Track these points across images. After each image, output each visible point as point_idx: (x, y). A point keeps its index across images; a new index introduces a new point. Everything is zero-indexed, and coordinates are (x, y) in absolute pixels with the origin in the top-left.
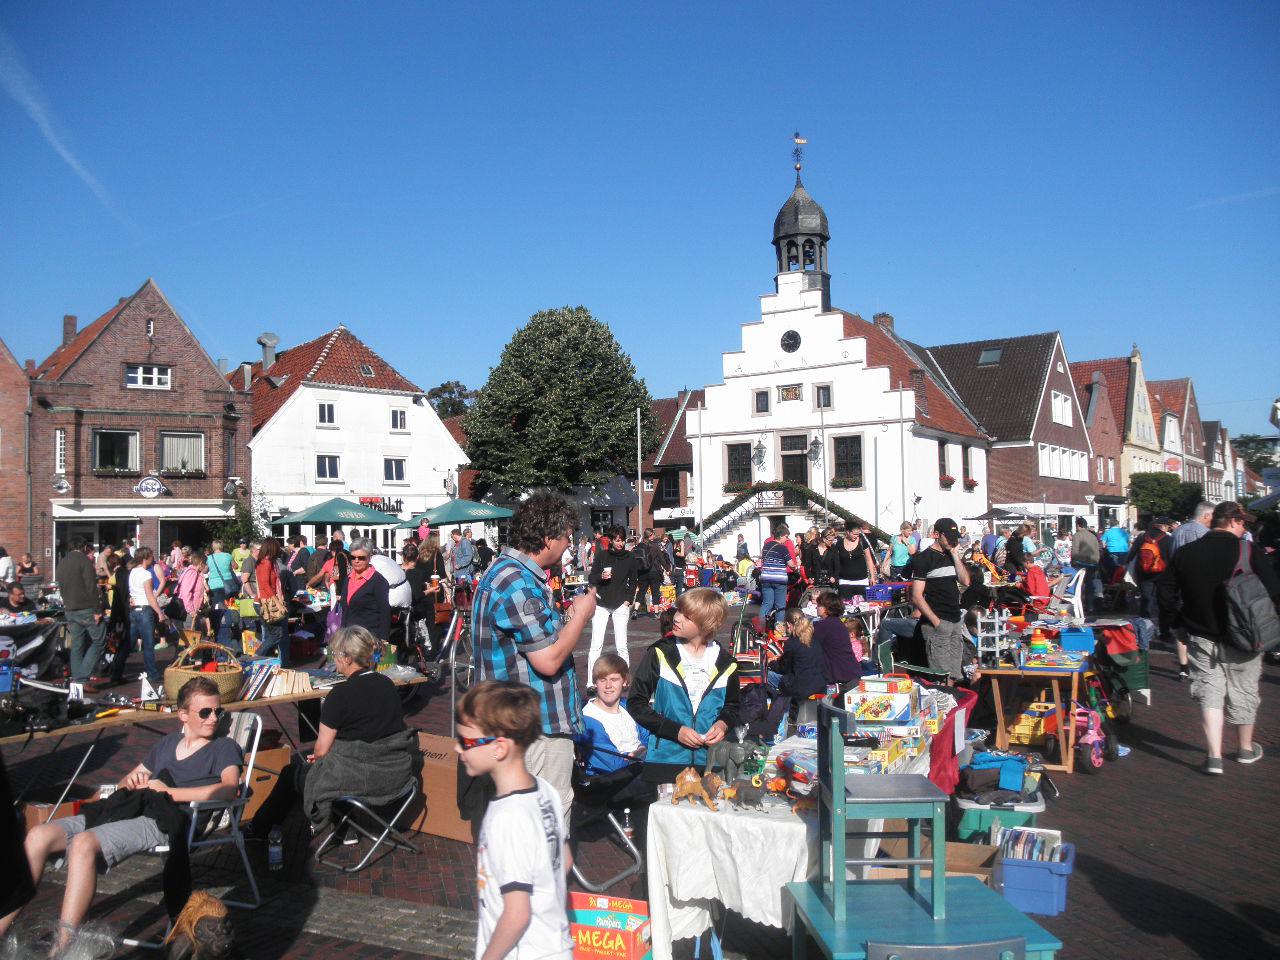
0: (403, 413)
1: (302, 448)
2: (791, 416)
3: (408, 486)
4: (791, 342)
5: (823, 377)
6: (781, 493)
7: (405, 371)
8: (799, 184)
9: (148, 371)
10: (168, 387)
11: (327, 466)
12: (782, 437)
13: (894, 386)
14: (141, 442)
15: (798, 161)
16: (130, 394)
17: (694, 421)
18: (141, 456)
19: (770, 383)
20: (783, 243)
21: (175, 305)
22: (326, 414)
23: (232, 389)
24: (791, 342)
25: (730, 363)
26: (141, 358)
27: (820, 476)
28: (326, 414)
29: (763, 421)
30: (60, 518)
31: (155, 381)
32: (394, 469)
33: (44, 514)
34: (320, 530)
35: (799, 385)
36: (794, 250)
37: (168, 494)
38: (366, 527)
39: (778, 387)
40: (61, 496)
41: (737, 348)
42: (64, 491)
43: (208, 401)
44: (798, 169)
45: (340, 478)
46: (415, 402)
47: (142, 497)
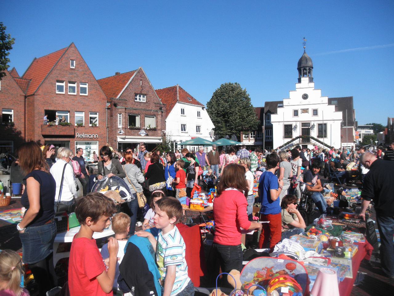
0: (200, 112)
1: (178, 122)
3: (202, 134)
4: (305, 97)
5: (315, 107)
6: (301, 139)
7: (198, 100)
9: (140, 96)
10: (145, 101)
11: (183, 128)
12: (302, 123)
14: (140, 119)
16: (136, 103)
17: (273, 117)
18: (140, 123)
19: (299, 108)
21: (148, 76)
22: (183, 111)
23: (161, 103)
24: (305, 97)
26: (139, 93)
27: (314, 133)
28: (183, 111)
29: (296, 118)
30: (120, 142)
31: (138, 99)
32: (198, 129)
33: (115, 141)
34: (182, 145)
35: (308, 109)
37: (147, 135)
38: (194, 146)
39: (301, 109)
40: (121, 135)
41: (288, 98)
42: (122, 133)
43: (156, 106)
44: (305, 48)
45: (201, 132)
46: (202, 109)
47: (141, 136)
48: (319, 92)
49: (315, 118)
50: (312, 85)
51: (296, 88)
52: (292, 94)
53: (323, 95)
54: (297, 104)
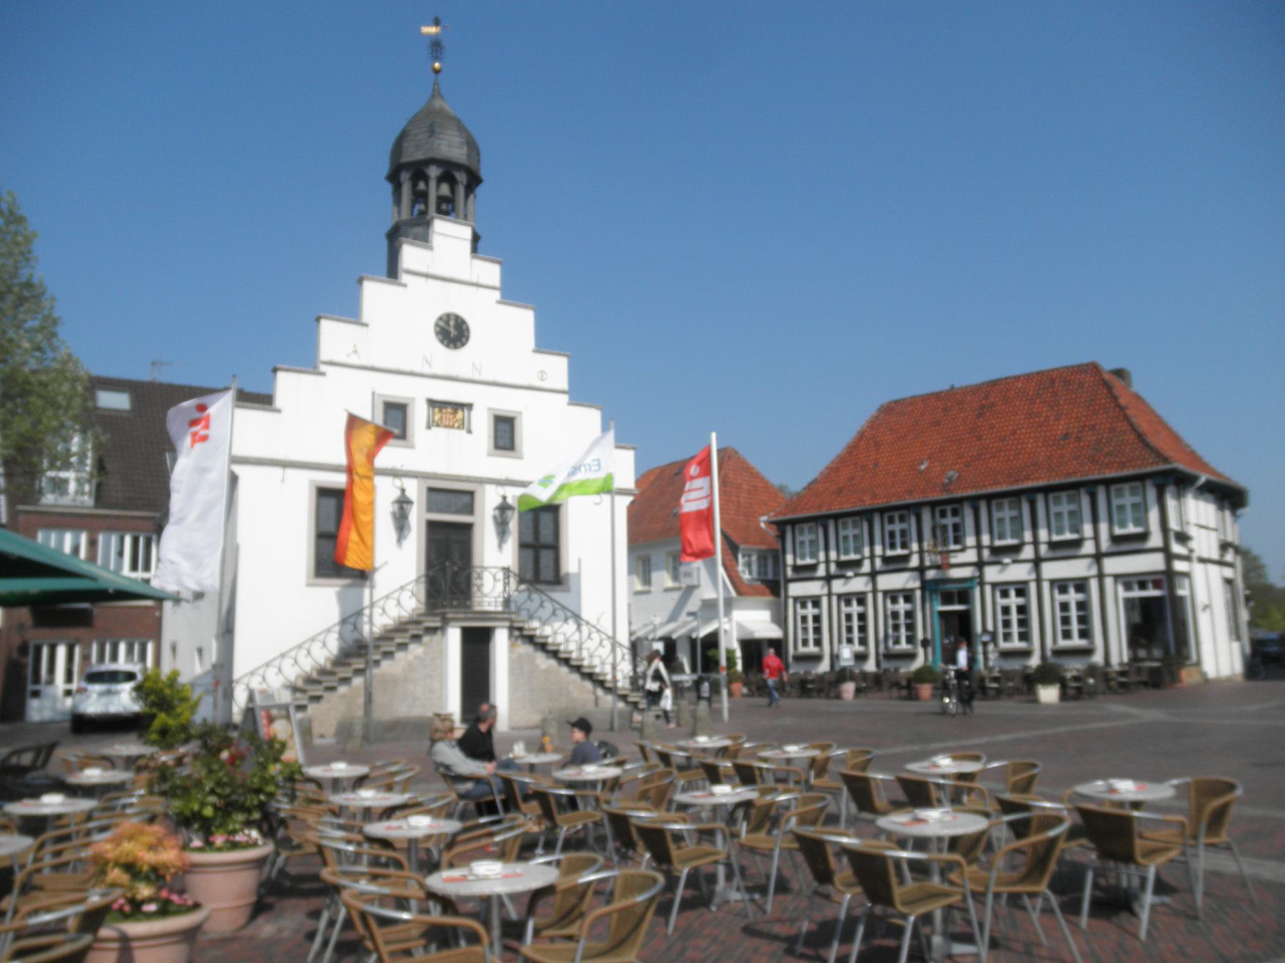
2: (435, 452)
4: (453, 332)
5: (507, 402)
8: (436, 93)
12: (431, 490)
15: (436, 59)
19: (416, 394)
20: (405, 177)
25: (334, 337)
27: (495, 556)
36: (422, 186)
41: (351, 312)
44: (437, 72)
49: (503, 466)
50: (491, 272)
52: (375, 293)
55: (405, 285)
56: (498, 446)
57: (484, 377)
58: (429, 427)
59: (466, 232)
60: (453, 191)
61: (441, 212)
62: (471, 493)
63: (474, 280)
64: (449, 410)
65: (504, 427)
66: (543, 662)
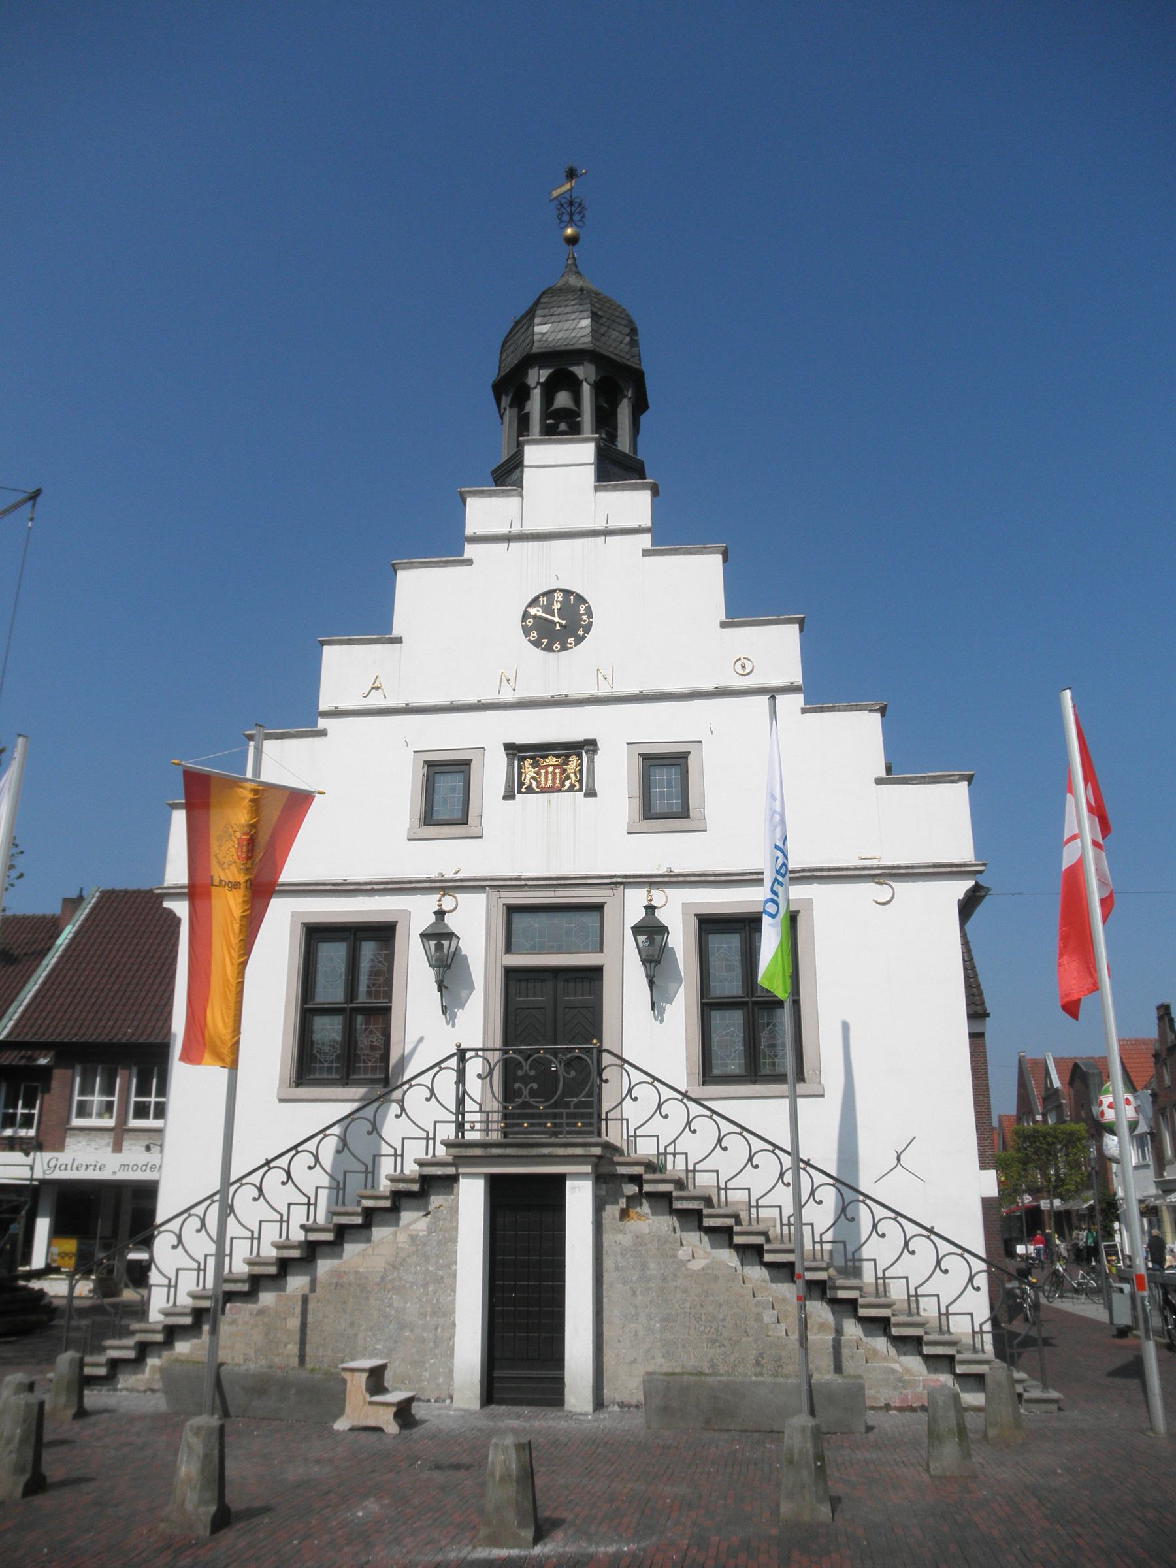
4: (559, 623)
5: (663, 727)
12: (512, 910)
13: (895, 772)
15: (571, 222)
19: (485, 739)
24: (559, 623)
25: (344, 671)
35: (590, 746)
41: (373, 622)
48: (704, 573)
50: (633, 505)
51: (469, 531)
53: (744, 606)
54: (472, 699)
55: (469, 562)
56: (649, 812)
57: (621, 689)
58: (509, 796)
59: (584, 451)
60: (577, 398)
61: (550, 432)
62: (598, 908)
63: (600, 525)
64: (551, 760)
65: (673, 775)
66: (698, 1252)
